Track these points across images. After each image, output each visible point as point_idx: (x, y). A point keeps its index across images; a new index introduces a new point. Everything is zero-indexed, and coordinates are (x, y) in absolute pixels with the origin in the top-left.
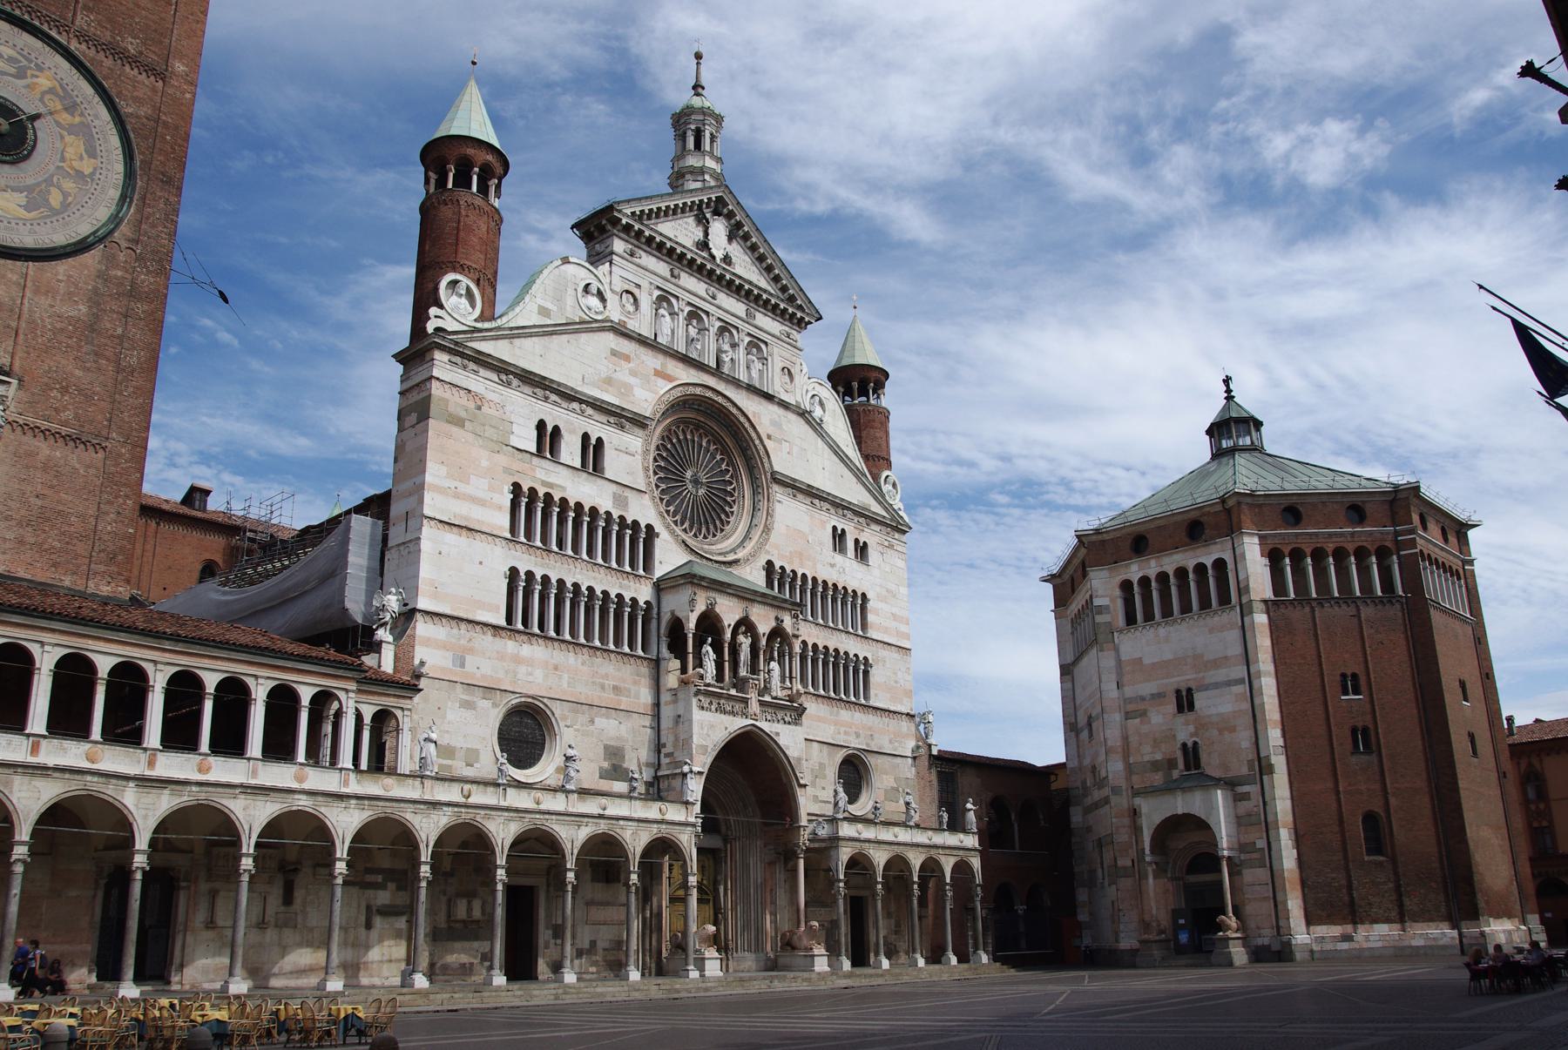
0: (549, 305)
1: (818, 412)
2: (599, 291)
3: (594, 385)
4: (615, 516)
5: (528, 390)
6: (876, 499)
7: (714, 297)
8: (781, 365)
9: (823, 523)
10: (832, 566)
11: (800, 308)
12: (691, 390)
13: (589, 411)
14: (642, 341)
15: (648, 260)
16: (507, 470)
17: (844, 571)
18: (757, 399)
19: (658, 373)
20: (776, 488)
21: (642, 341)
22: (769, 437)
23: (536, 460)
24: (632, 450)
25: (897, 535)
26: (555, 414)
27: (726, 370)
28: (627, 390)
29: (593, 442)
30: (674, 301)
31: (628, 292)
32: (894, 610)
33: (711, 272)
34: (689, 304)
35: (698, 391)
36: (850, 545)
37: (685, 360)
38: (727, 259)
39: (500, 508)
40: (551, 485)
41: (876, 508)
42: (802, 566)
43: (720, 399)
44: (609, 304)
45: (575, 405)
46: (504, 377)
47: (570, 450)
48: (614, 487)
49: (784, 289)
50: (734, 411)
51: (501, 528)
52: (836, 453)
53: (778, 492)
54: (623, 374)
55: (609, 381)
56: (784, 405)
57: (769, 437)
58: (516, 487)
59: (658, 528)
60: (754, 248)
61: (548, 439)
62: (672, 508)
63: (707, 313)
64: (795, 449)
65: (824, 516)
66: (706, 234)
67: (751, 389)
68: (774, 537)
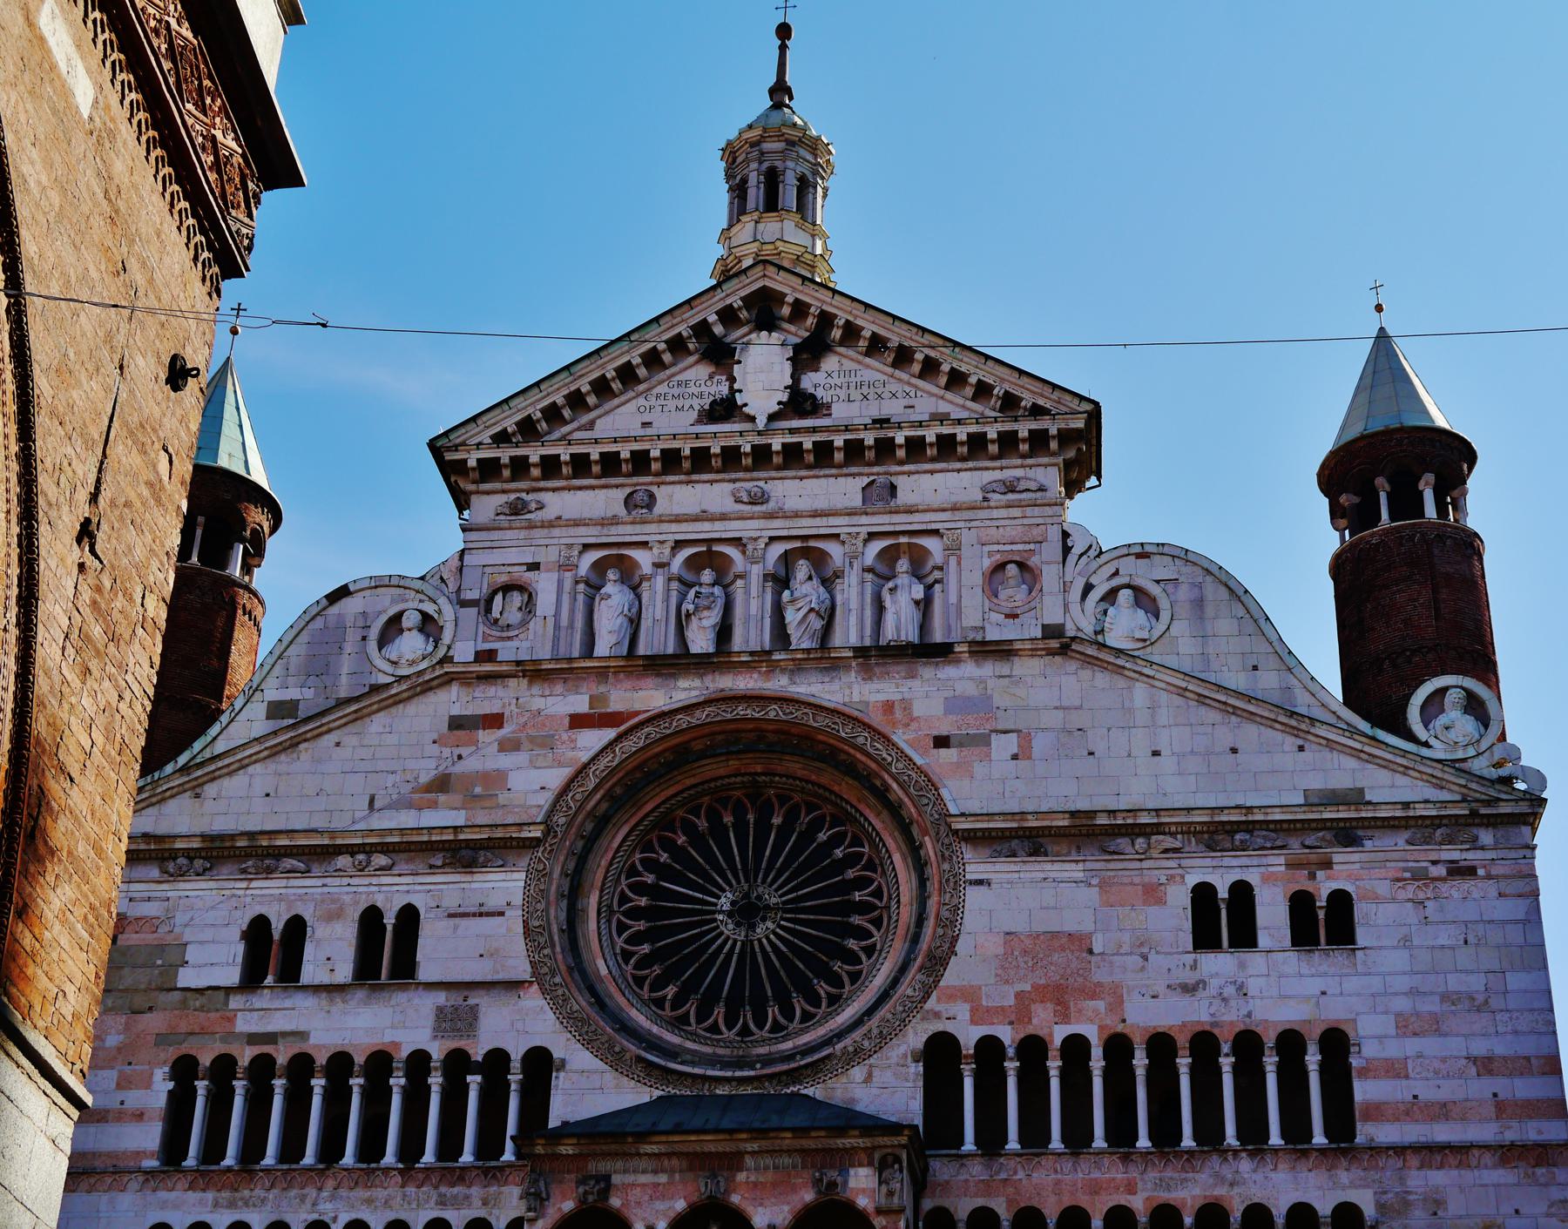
0: (292, 694)
1: (1124, 625)
2: (426, 617)
3: (396, 805)
4: (437, 1052)
5: (226, 870)
6: (1386, 765)
7: (759, 499)
8: (987, 563)
9: (1153, 895)
10: (1189, 989)
11: (1037, 411)
12: (683, 721)
13: (381, 860)
14: (533, 672)
15: (562, 502)
16: (162, 1040)
17: (1275, 987)
18: (898, 670)
19: (578, 722)
20: (968, 853)
21: (533, 672)
22: (941, 742)
23: (236, 1002)
24: (494, 902)
25: (1486, 837)
26: (274, 897)
27: (801, 639)
28: (497, 779)
29: (389, 920)
30: (637, 554)
31: (507, 589)
32: (1480, 1048)
33: (731, 457)
34: (679, 545)
35: (701, 716)
36: (1272, 914)
37: (679, 662)
38: (800, 403)
39: (139, 1116)
40: (271, 1038)
41: (1388, 788)
42: (1065, 1018)
43: (773, 712)
44: (447, 637)
45: (343, 861)
46: (171, 867)
47: (330, 952)
48: (441, 998)
49: (983, 391)
50: (821, 722)
51: (139, 1154)
52: (1201, 699)
53: (975, 865)
54: (484, 755)
55: (442, 784)
56: (1001, 651)
57: (941, 742)
58: (184, 1070)
59: (562, 1045)
60: (876, 345)
61: (272, 953)
62: (671, 991)
63: (737, 542)
64: (1040, 744)
65: (1157, 870)
66: (796, 377)
67: (878, 655)
68: (952, 976)
